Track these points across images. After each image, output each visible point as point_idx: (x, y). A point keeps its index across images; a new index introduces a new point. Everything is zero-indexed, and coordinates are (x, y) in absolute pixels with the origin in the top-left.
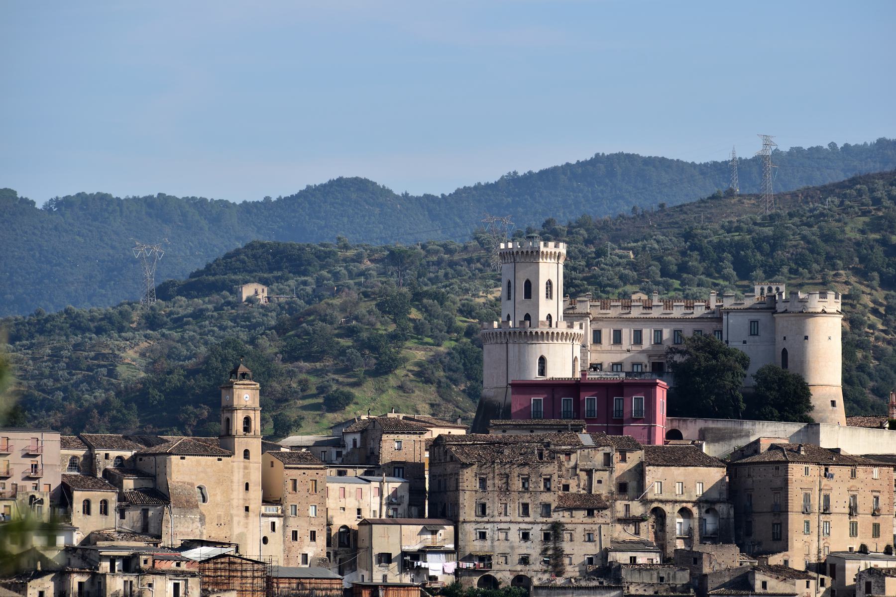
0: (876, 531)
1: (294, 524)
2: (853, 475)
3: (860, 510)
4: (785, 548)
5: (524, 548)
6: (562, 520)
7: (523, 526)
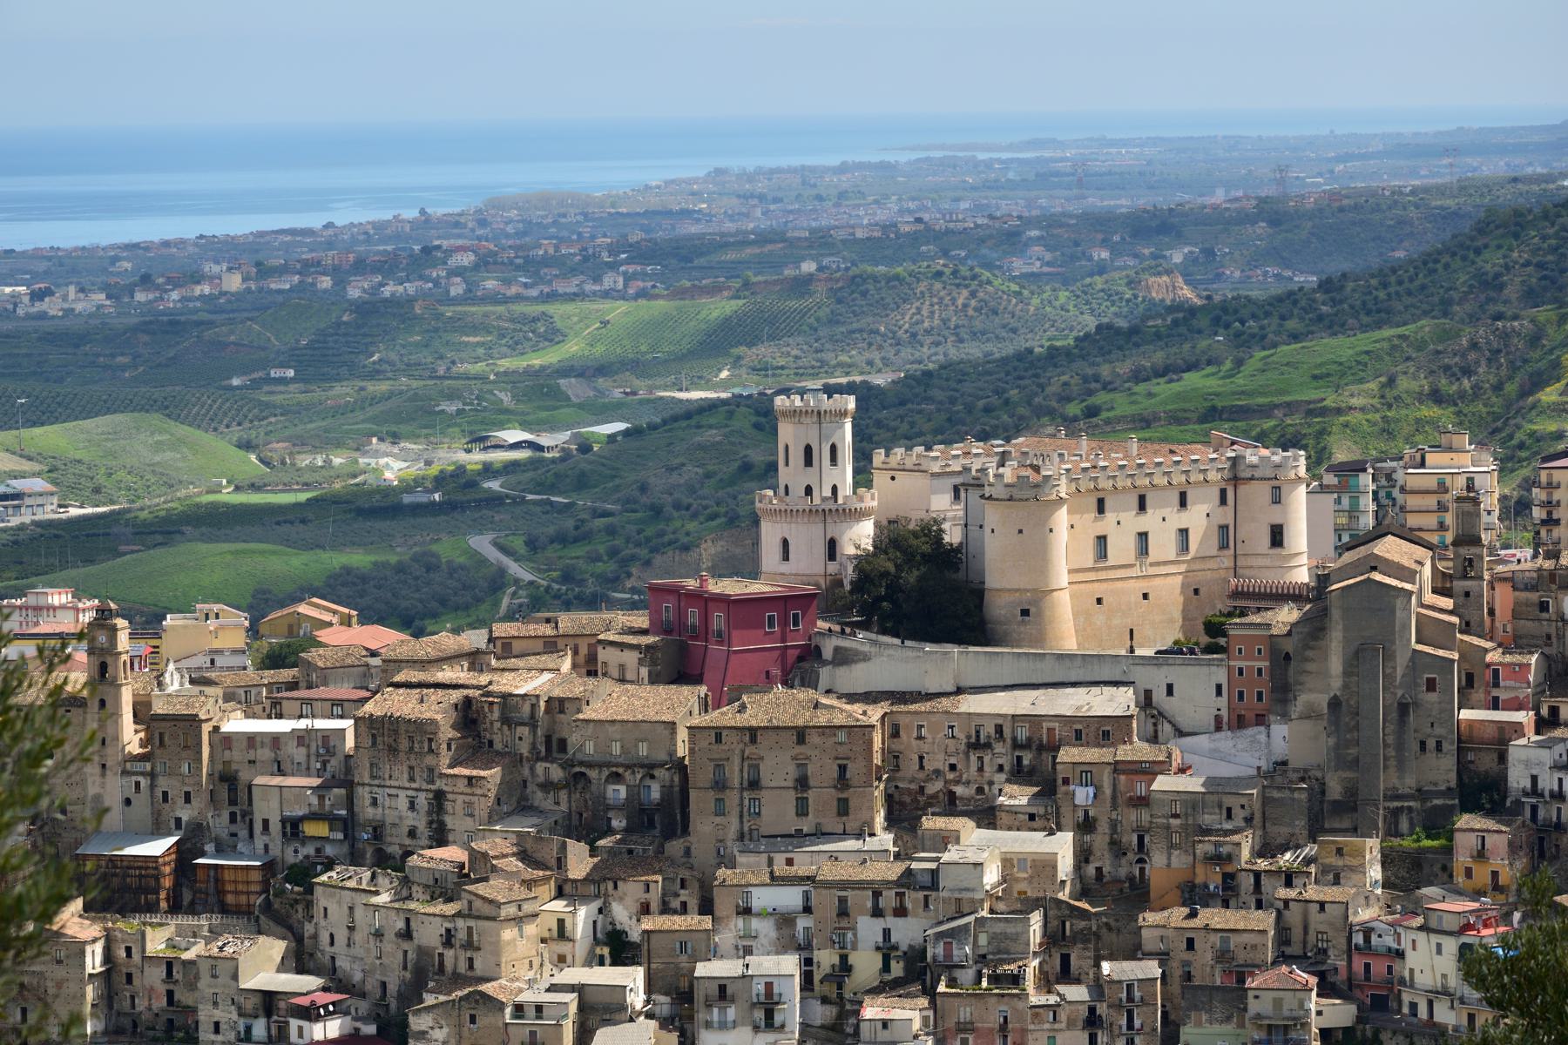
3: (812, 782)
4: (685, 831)
5: (410, 819)
6: (445, 788)
7: (410, 793)
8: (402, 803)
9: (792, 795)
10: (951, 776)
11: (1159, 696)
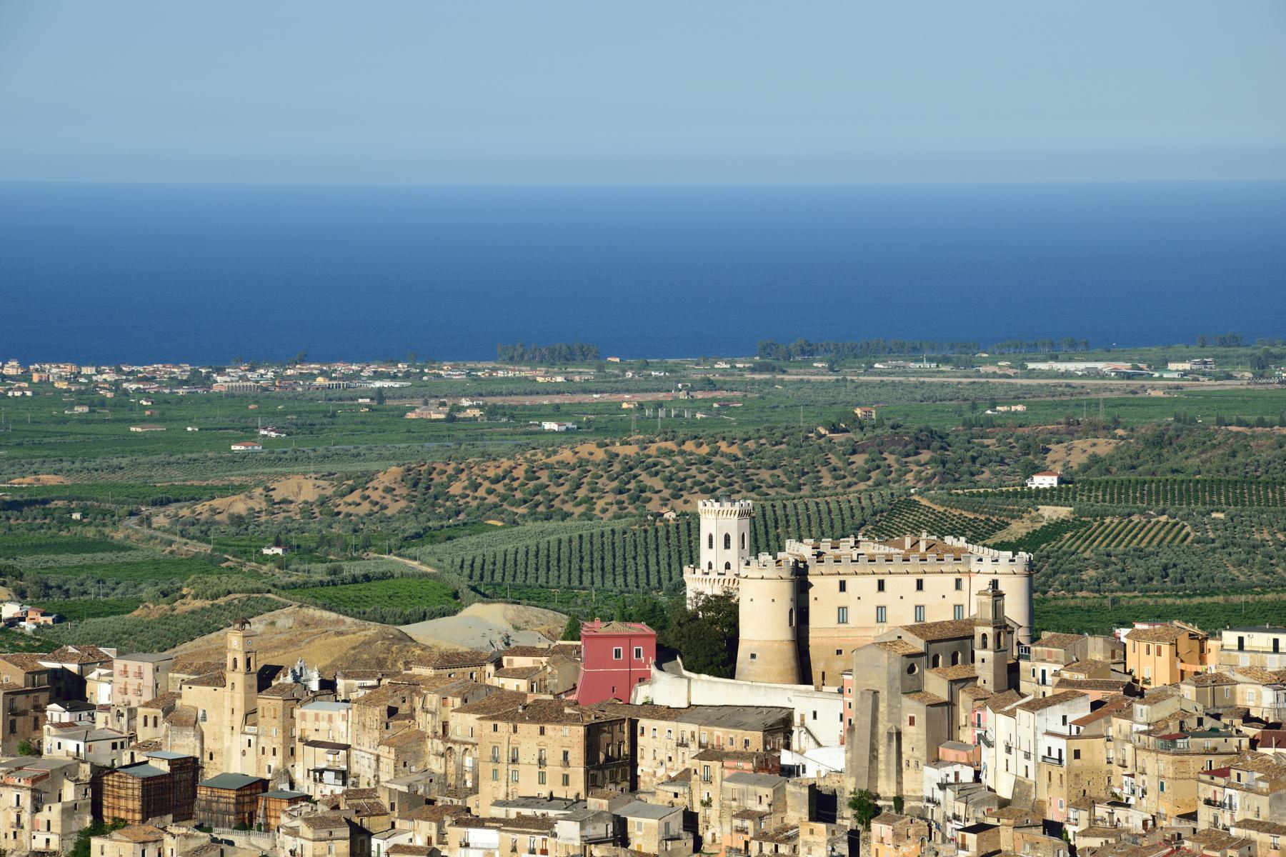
0: (566, 780)
1: (263, 742)
2: (542, 732)
3: (548, 762)
8: (366, 762)
9: (536, 769)
10: (669, 765)
11: (809, 721)
